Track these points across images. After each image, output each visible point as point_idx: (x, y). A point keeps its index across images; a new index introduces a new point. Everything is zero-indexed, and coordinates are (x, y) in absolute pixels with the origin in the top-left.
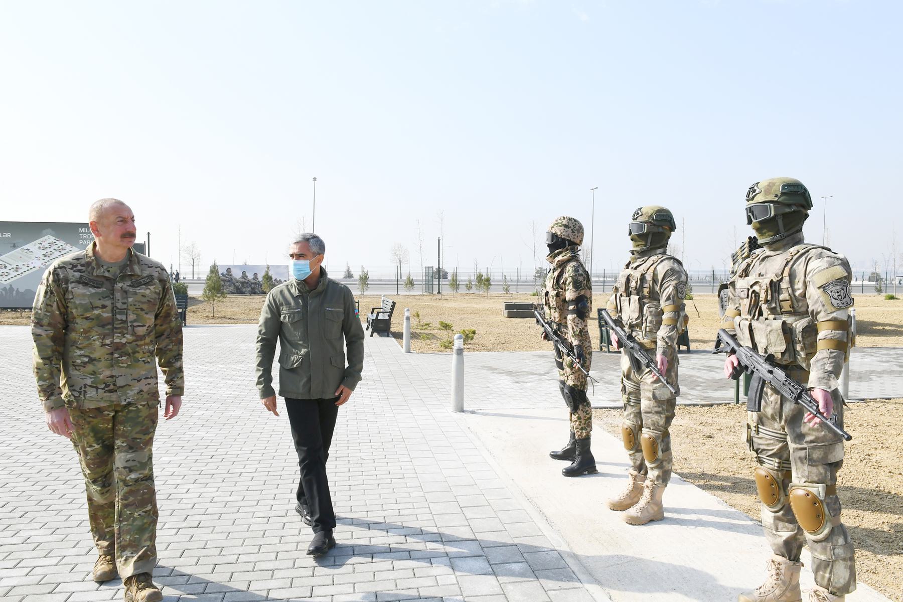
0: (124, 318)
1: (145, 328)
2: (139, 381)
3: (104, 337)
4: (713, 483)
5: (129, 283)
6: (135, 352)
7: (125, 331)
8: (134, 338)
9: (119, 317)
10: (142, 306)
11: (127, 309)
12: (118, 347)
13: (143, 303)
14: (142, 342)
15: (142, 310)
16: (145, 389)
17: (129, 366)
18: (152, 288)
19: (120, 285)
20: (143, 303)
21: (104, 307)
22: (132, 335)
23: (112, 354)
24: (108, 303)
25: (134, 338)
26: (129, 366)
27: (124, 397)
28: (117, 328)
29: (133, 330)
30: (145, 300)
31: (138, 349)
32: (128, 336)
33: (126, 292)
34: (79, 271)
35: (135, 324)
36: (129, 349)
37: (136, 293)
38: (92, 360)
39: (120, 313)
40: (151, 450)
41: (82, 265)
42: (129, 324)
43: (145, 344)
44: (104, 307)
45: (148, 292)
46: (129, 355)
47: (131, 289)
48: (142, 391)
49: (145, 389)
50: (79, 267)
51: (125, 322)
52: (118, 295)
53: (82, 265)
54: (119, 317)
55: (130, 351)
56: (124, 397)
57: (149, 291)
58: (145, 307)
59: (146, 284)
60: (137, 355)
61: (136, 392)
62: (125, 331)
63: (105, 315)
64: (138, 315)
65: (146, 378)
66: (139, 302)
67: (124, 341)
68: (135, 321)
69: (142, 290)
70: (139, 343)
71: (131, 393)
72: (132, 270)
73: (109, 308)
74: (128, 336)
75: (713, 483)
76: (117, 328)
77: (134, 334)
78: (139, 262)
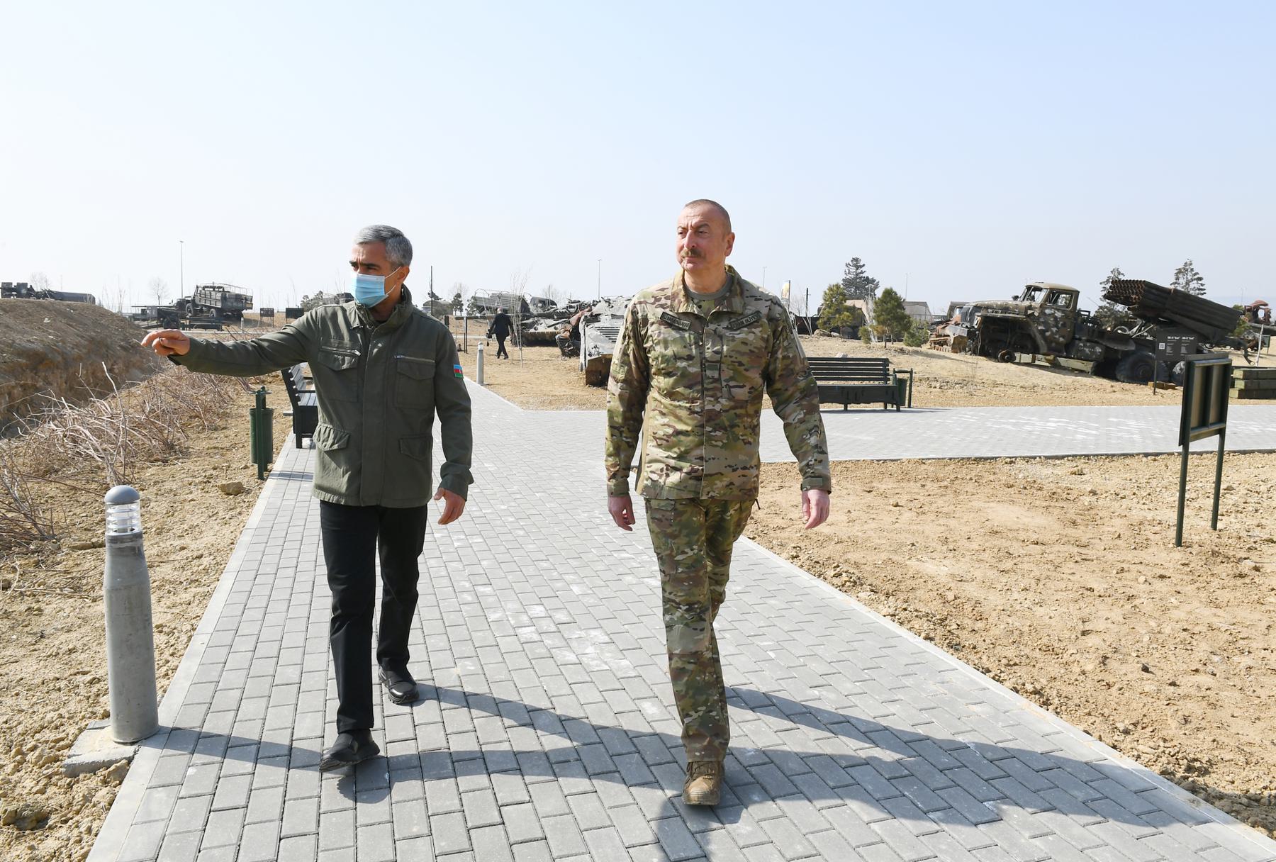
0: (716, 376)
1: (746, 390)
5: (725, 324)
9: (709, 373)
10: (740, 359)
11: (720, 362)
13: (743, 354)
15: (741, 364)
16: (737, 482)
18: (757, 331)
19: (712, 327)
20: (743, 354)
22: (729, 399)
28: (708, 390)
30: (744, 349)
32: (723, 401)
33: (721, 337)
35: (732, 384)
37: (733, 339)
39: (711, 368)
45: (751, 337)
47: (728, 333)
48: (732, 484)
49: (737, 482)
51: (718, 380)
54: (709, 373)
56: (707, 489)
57: (754, 336)
58: (745, 360)
59: (749, 325)
63: (693, 370)
64: (735, 370)
66: (738, 352)
67: (718, 407)
68: (732, 379)
69: (741, 335)
71: (719, 484)
72: (730, 305)
74: (723, 401)
76: (708, 390)
77: (731, 398)
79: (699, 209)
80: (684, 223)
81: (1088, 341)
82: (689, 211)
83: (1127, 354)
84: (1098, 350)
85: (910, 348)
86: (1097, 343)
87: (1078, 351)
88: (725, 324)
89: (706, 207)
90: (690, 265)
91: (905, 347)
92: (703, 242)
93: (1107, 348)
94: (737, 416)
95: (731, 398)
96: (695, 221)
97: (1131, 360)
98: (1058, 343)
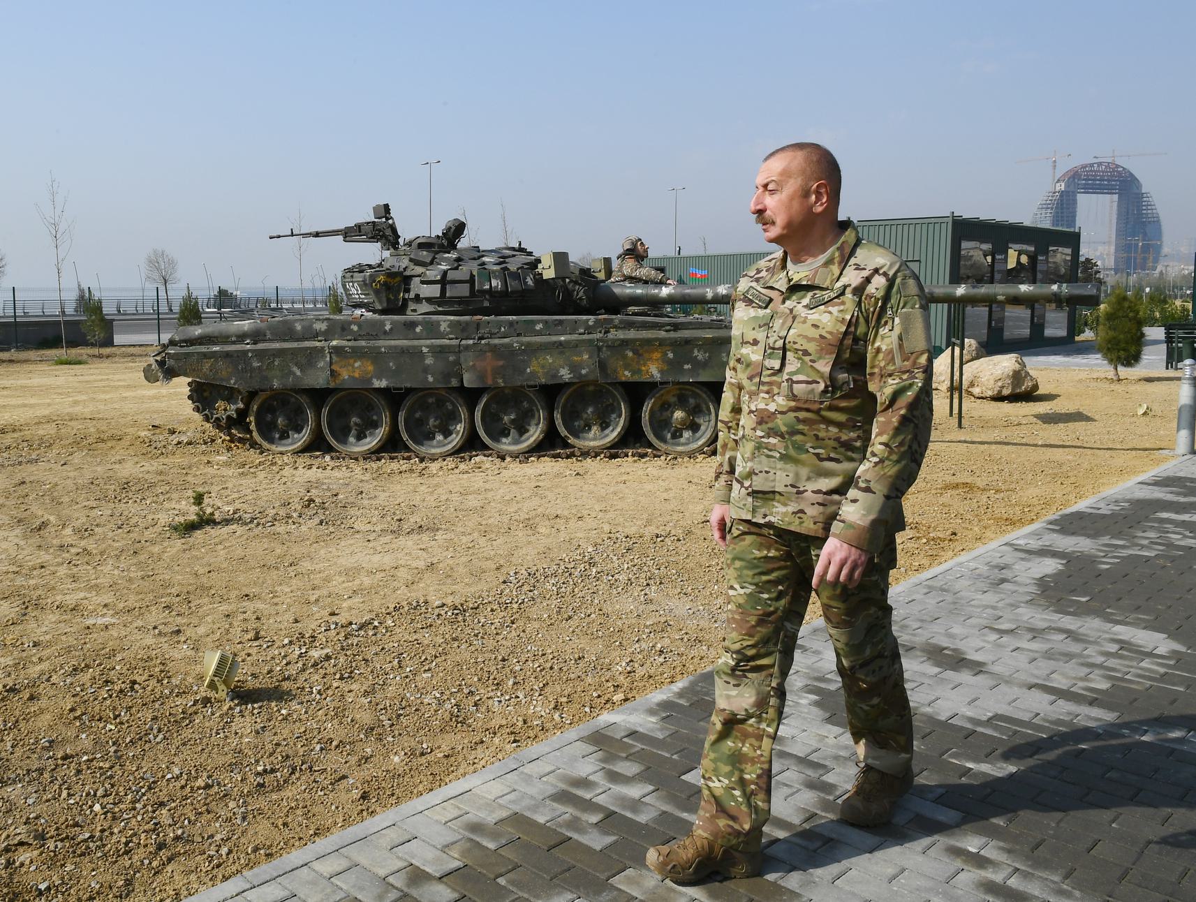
2: (799, 493)
5: (806, 301)
6: (793, 433)
7: (776, 391)
8: (793, 404)
12: (763, 419)
13: (810, 340)
15: (806, 353)
17: (784, 458)
18: (835, 310)
21: (755, 342)
22: (787, 397)
23: (754, 429)
24: (761, 335)
25: (793, 404)
28: (764, 384)
30: (815, 333)
35: (795, 378)
36: (781, 423)
39: (770, 356)
42: (785, 377)
52: (777, 324)
55: (784, 429)
58: (811, 347)
60: (798, 438)
61: (790, 509)
62: (776, 391)
66: (806, 337)
69: (815, 316)
70: (802, 415)
73: (761, 346)
76: (764, 384)
77: (794, 397)
88: (806, 301)
95: (794, 397)
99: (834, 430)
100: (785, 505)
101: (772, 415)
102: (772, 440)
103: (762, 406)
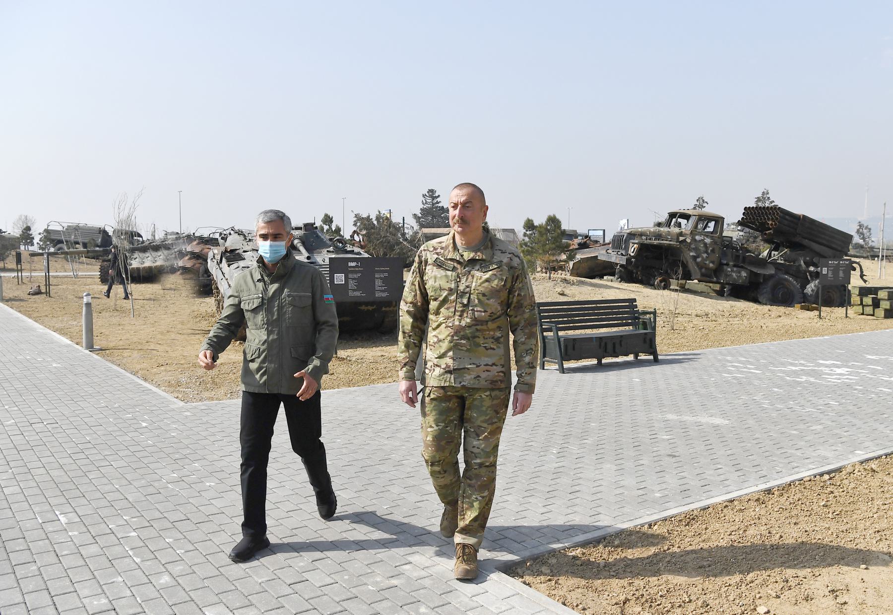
2: (478, 366)
3: (448, 318)
4: (632, 554)
6: (474, 337)
14: (484, 327)
17: (468, 350)
26: (468, 350)
27: (460, 380)
29: (473, 314)
31: (477, 334)
34: (437, 254)
38: (439, 341)
39: (462, 297)
40: (498, 439)
41: (442, 248)
43: (489, 330)
44: (451, 290)
46: (468, 339)
48: (479, 376)
49: (484, 375)
50: (439, 251)
53: (442, 248)
55: (469, 335)
56: (460, 380)
60: (477, 340)
61: (473, 377)
65: (487, 365)
67: (463, 323)
70: (478, 327)
74: (468, 320)
75: (632, 554)
78: (492, 247)
79: (465, 191)
80: (455, 200)
81: (735, 266)
82: (457, 191)
83: (767, 278)
84: (744, 274)
85: (572, 278)
86: (742, 267)
87: (727, 276)
89: (470, 189)
90: (460, 229)
91: (568, 277)
92: (468, 213)
93: (751, 271)
94: (477, 330)
96: (463, 199)
97: (771, 283)
98: (707, 268)
99: (492, 333)
100: (470, 374)
101: (463, 328)
102: (463, 342)
103: (457, 323)
